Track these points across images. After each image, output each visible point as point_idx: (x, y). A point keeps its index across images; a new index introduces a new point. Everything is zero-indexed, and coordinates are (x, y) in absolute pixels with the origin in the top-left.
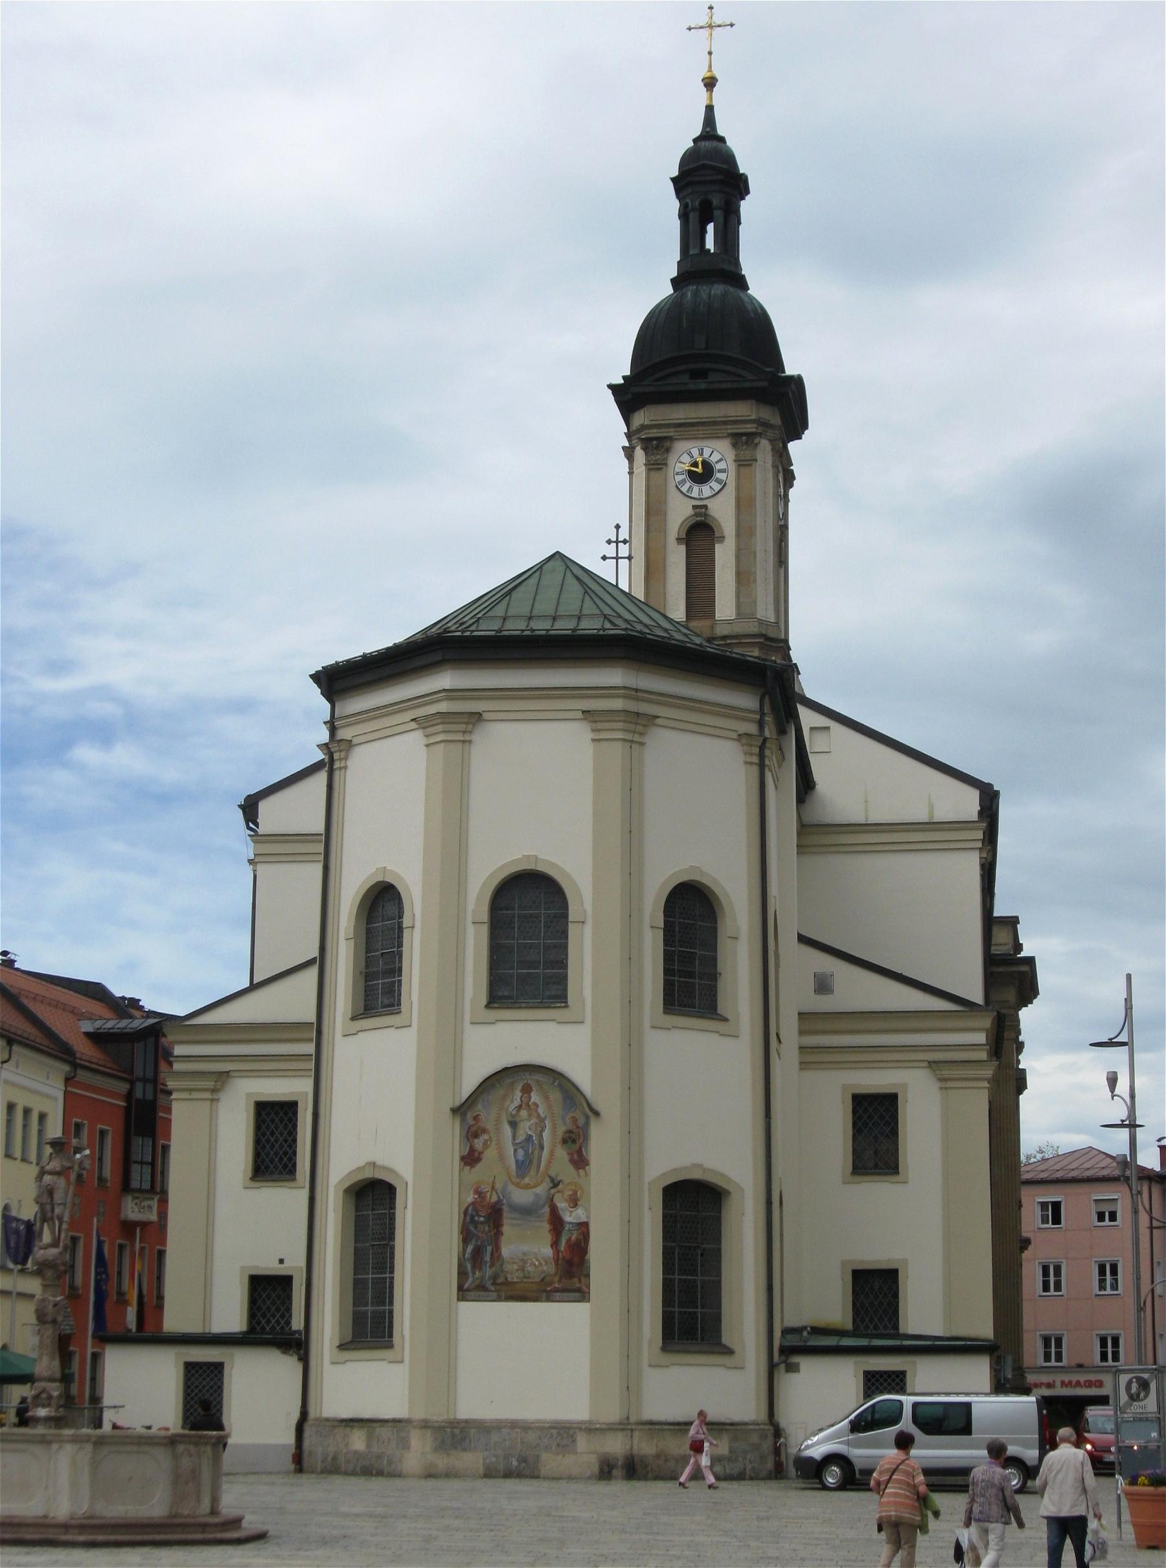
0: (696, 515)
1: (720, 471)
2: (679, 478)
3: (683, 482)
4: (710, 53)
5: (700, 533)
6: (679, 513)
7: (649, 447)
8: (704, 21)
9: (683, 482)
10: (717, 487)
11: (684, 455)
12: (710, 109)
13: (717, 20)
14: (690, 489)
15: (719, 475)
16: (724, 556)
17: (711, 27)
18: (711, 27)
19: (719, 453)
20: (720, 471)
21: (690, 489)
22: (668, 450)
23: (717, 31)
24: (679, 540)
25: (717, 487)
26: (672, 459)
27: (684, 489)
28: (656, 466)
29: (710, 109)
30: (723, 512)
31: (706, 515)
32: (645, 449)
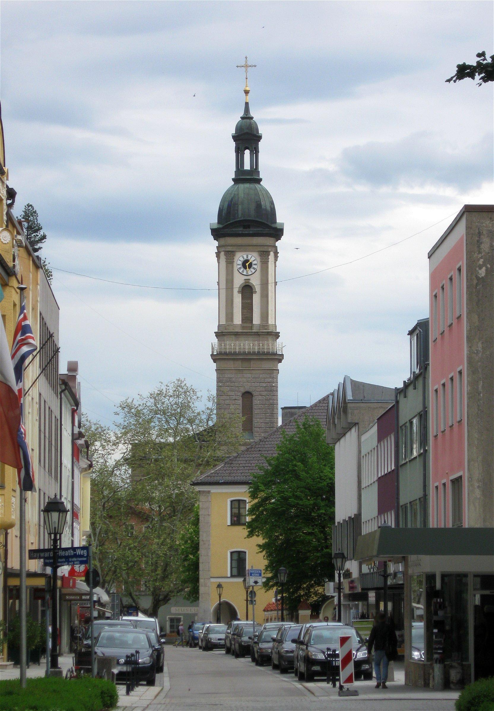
0: (246, 282)
1: (255, 264)
2: (239, 266)
3: (240, 268)
4: (247, 78)
5: (247, 290)
6: (239, 281)
7: (226, 254)
8: (243, 63)
9: (240, 268)
10: (253, 271)
11: (239, 258)
12: (247, 104)
13: (249, 63)
14: (243, 271)
15: (254, 266)
16: (256, 299)
17: (246, 66)
18: (246, 66)
19: (254, 257)
20: (256, 264)
21: (243, 271)
22: (234, 255)
23: (249, 69)
24: (239, 292)
25: (253, 271)
26: (235, 260)
27: (241, 271)
28: (230, 262)
29: (247, 104)
30: (255, 281)
31: (249, 282)
32: (225, 255)
